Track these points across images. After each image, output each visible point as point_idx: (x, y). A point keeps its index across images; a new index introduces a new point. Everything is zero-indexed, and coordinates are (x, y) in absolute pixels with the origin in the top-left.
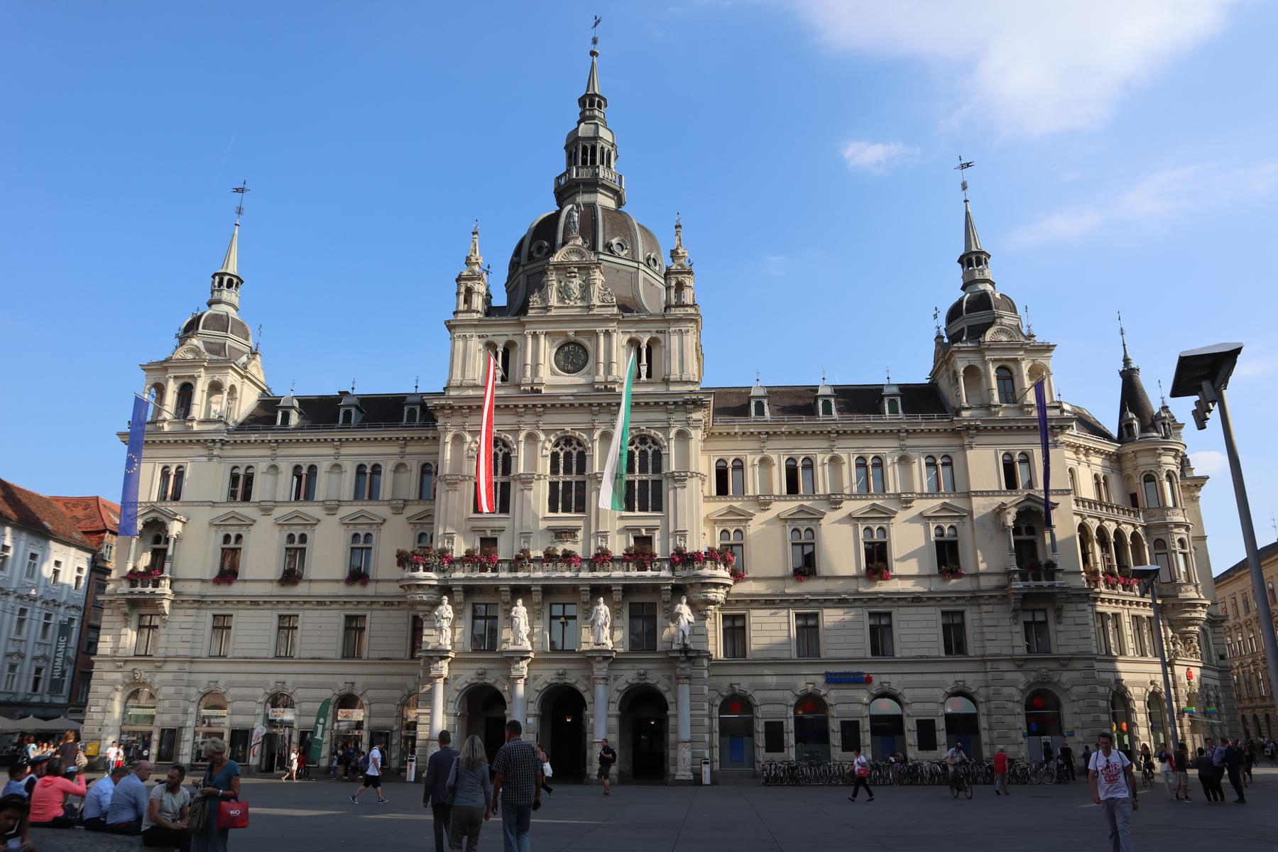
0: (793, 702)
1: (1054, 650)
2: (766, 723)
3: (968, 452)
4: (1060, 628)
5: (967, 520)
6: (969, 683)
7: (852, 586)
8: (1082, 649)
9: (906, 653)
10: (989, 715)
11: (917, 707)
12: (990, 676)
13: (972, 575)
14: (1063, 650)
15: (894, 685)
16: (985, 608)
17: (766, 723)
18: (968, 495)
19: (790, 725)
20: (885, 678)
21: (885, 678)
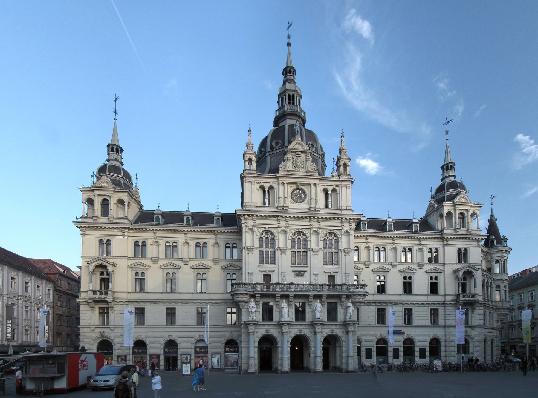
0: (376, 341)
1: (470, 324)
2: (366, 349)
3: (446, 247)
4: (473, 316)
5: (442, 274)
6: (438, 335)
7: (397, 298)
8: (480, 324)
9: (417, 324)
10: (446, 346)
11: (419, 343)
12: (447, 332)
13: (442, 295)
14: (473, 324)
15: (412, 335)
16: (447, 308)
17: (366, 349)
18: (444, 264)
19: (374, 349)
20: (409, 333)
21: (409, 333)
